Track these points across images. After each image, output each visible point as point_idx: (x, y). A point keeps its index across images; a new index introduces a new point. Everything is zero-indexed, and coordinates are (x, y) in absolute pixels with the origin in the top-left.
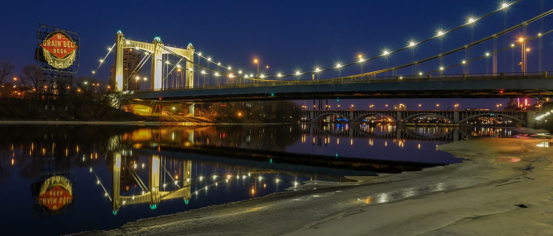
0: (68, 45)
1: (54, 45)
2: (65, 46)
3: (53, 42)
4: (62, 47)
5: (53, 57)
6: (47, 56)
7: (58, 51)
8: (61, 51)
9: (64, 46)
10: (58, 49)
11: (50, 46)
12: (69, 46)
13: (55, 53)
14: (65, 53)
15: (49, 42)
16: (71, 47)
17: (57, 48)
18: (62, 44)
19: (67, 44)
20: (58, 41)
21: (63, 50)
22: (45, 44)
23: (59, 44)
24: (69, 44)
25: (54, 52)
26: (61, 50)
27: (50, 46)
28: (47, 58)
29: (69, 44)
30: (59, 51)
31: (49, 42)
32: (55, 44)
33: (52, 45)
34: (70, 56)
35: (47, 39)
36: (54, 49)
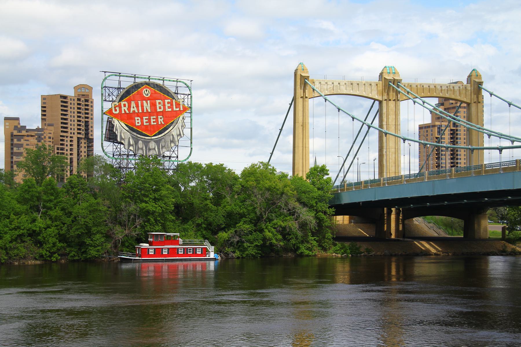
0: (167, 108)
1: (135, 109)
2: (161, 110)
3: (133, 104)
4: (154, 112)
5: (135, 134)
6: (121, 133)
7: (145, 121)
8: (152, 120)
9: (158, 110)
10: (144, 118)
11: (127, 112)
12: (169, 107)
13: (140, 124)
14: (160, 123)
15: (125, 105)
16: (173, 109)
17: (141, 115)
18: (153, 105)
19: (164, 105)
20: (144, 102)
21: (157, 119)
22: (116, 110)
23: (147, 106)
24: (169, 105)
25: (137, 124)
26: (152, 117)
27: (127, 112)
28: (121, 136)
29: (169, 105)
30: (147, 121)
31: (125, 105)
32: (137, 106)
33: (132, 109)
34: (171, 127)
35: (121, 100)
36: (136, 118)
